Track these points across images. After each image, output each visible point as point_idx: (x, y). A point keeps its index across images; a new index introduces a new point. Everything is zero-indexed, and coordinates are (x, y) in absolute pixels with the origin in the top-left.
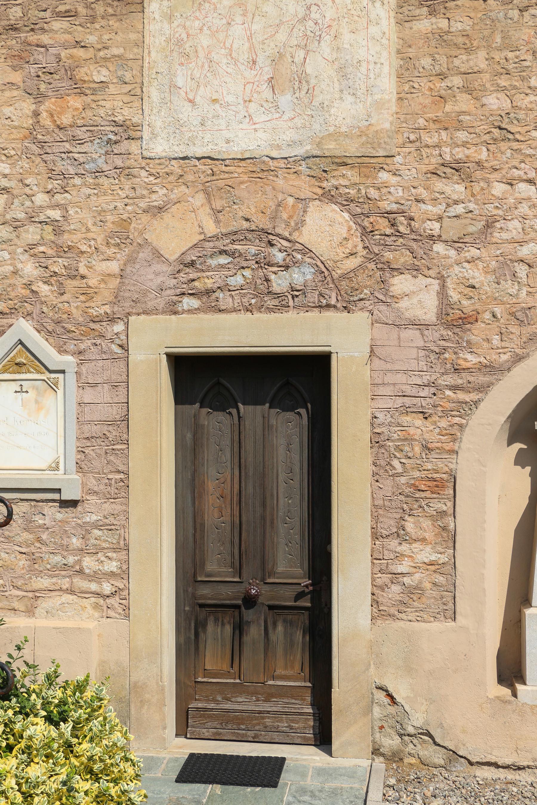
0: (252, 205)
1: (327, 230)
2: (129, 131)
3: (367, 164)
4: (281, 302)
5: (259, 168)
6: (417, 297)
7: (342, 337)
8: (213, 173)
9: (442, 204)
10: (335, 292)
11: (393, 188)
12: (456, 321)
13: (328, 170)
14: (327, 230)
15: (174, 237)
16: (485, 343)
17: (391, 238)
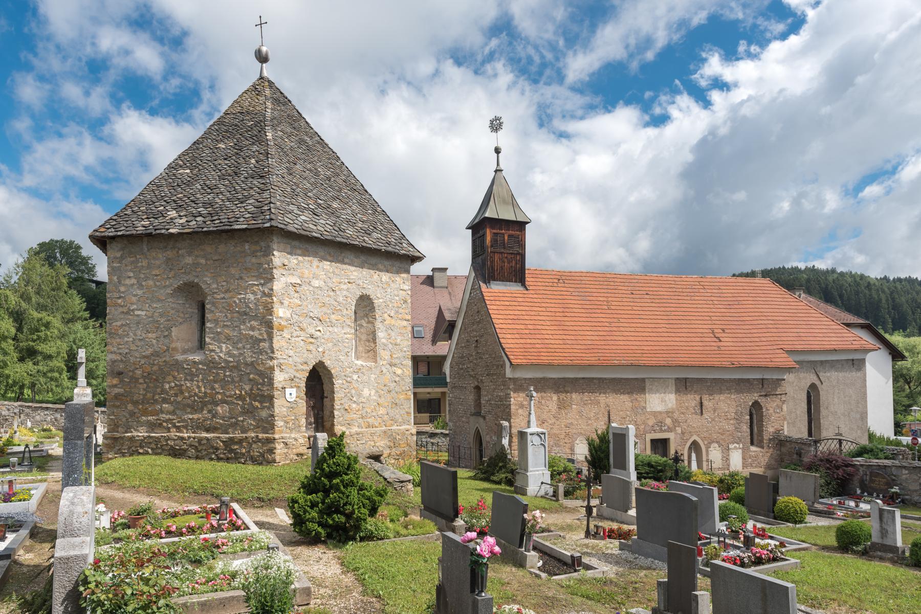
0: (660, 418)
1: (668, 421)
2: (645, 408)
3: (673, 413)
4: (665, 431)
5: (660, 413)
6: (679, 430)
7: (670, 436)
8: (655, 414)
9: (682, 418)
10: (670, 430)
11: (676, 415)
12: (683, 433)
13: (669, 413)
14: (668, 421)
15: (651, 422)
16: (686, 436)
17: (676, 422)
